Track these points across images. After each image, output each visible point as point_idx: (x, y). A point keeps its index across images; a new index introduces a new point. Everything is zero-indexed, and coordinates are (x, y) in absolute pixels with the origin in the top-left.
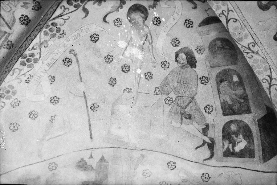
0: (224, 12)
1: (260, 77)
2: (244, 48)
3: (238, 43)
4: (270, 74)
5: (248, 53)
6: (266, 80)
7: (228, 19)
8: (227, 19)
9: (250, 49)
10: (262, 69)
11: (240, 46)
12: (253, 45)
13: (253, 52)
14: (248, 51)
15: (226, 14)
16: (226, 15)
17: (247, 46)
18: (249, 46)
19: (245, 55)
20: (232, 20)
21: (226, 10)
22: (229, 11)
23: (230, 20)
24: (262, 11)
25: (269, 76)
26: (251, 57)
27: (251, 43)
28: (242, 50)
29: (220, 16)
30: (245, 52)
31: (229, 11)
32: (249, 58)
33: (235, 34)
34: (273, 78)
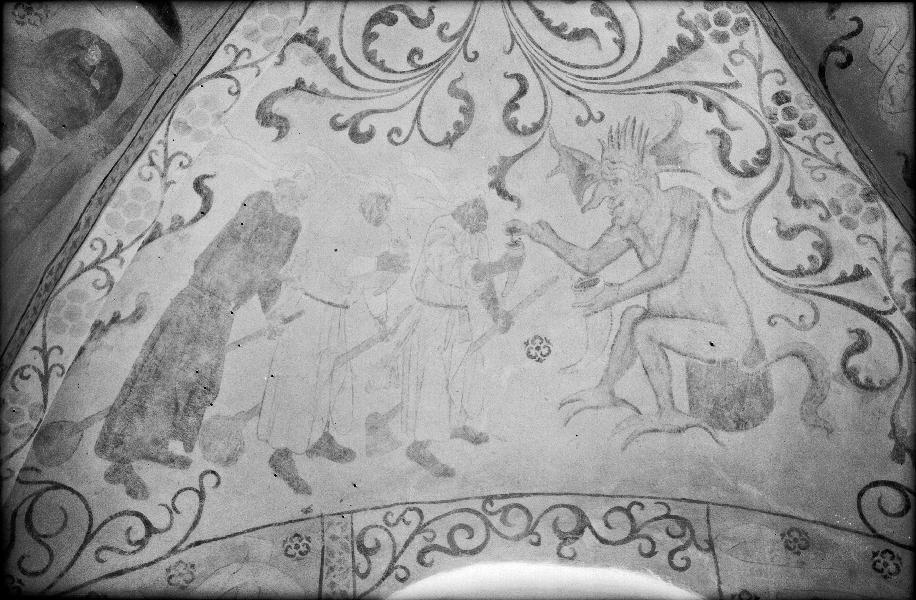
0: (246, 53)
1: (100, 230)
2: (161, 148)
3: (168, 129)
4: (126, 243)
5: (152, 164)
6: (105, 245)
7: (228, 73)
8: (229, 68)
9: (167, 162)
10: (127, 221)
11: (159, 135)
12: (186, 163)
13: (163, 175)
14: (159, 160)
15: (243, 60)
16: (238, 64)
17: (170, 153)
18: (173, 156)
19: (144, 159)
20: (231, 82)
21: (256, 56)
22: (252, 65)
23: (229, 77)
24: (254, 114)
25: (120, 245)
26: (147, 176)
27: (186, 155)
28: (153, 145)
29: (226, 48)
30: (150, 158)
31: (252, 65)
32: (140, 174)
33: (192, 106)
34: (122, 255)
